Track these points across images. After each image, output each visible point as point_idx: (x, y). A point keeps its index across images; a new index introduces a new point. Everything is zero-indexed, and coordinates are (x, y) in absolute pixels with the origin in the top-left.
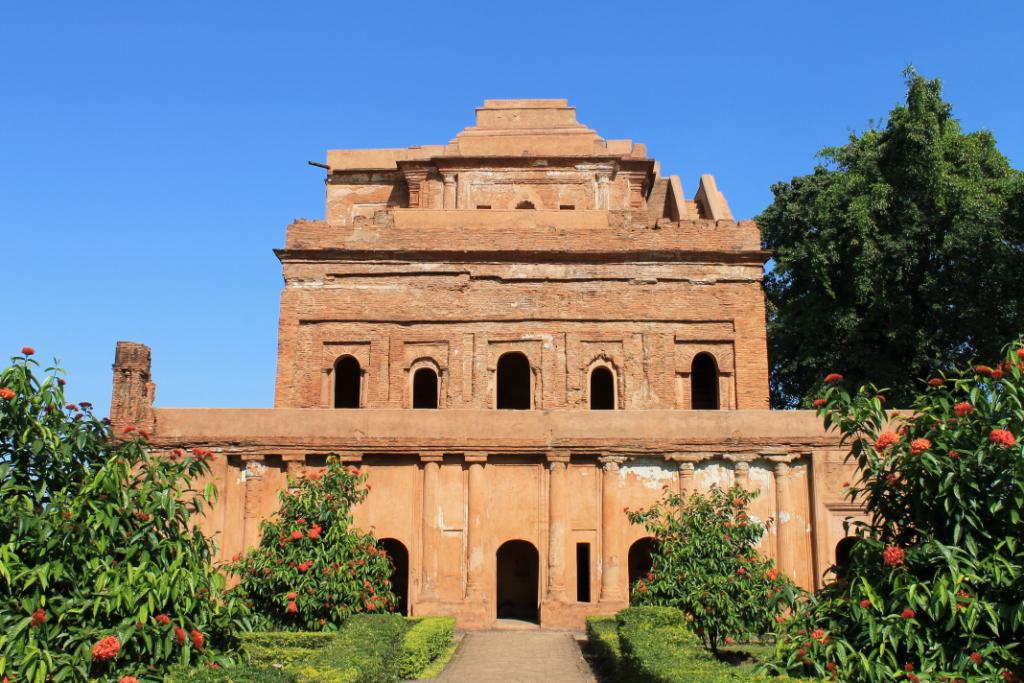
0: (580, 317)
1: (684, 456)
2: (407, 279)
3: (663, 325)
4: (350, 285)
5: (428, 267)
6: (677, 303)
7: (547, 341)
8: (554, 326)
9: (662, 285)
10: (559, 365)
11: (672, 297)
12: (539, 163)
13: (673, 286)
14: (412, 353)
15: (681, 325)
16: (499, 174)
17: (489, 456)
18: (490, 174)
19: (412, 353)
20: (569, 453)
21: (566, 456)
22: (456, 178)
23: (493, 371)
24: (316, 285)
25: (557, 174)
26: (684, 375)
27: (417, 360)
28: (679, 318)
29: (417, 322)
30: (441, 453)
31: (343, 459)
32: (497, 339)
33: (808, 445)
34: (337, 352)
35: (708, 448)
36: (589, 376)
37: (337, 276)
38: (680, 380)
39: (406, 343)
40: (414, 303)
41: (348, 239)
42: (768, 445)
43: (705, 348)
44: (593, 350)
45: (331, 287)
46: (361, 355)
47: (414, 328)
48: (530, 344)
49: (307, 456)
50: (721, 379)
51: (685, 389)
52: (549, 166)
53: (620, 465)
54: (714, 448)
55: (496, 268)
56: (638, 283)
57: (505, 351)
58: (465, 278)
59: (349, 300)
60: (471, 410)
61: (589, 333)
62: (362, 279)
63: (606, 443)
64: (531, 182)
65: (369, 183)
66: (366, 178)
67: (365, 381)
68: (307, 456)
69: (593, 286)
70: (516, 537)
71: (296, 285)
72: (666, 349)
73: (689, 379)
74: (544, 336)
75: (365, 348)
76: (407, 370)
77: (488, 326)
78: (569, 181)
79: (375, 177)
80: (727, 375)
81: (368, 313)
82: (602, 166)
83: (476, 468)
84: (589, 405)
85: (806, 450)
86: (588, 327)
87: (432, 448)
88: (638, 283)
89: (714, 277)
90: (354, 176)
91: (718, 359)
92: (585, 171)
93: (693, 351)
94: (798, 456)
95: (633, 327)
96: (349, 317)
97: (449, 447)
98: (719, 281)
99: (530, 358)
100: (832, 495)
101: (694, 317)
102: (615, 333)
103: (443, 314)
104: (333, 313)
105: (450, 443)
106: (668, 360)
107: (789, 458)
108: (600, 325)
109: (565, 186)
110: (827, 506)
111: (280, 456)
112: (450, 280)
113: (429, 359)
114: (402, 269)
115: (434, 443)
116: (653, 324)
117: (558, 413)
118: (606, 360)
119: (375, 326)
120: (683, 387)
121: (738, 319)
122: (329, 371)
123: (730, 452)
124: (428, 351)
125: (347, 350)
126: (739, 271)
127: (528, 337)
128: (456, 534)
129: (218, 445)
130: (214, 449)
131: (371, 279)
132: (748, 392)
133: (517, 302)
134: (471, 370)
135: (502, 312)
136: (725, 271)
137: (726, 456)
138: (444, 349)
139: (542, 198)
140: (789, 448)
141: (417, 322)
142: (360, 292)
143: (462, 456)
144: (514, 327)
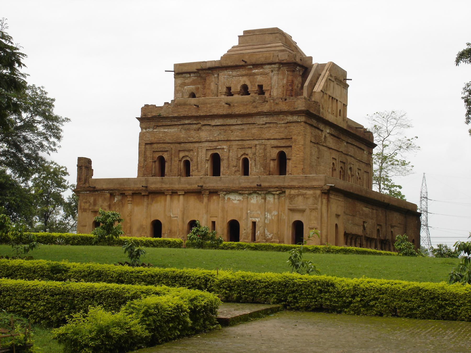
2: (180, 127)
3: (267, 141)
4: (162, 130)
5: (187, 122)
6: (273, 132)
7: (226, 148)
8: (228, 143)
9: (267, 125)
10: (230, 157)
11: (270, 130)
12: (249, 67)
13: (272, 125)
14: (182, 155)
15: (273, 141)
16: (235, 73)
18: (231, 73)
19: (182, 155)
20: (208, 191)
22: (218, 74)
23: (208, 160)
24: (151, 130)
25: (256, 71)
26: (274, 160)
27: (183, 157)
28: (272, 138)
29: (183, 143)
31: (142, 194)
32: (209, 148)
33: (284, 188)
34: (157, 155)
35: (251, 189)
36: (241, 161)
37: (157, 126)
38: (272, 162)
39: (180, 151)
40: (182, 136)
41: (161, 112)
42: (270, 188)
43: (282, 149)
45: (155, 130)
46: (166, 156)
47: (182, 145)
50: (287, 161)
51: (274, 165)
52: (253, 68)
53: (225, 195)
54: (254, 189)
55: (210, 121)
56: (259, 125)
57: (212, 153)
58: (199, 126)
59: (161, 135)
60: (201, 175)
62: (166, 128)
63: (219, 188)
64: (246, 75)
65: (190, 77)
66: (189, 75)
67: (166, 164)
69: (243, 127)
71: (144, 130)
72: (268, 150)
73: (276, 162)
74: (225, 147)
75: (166, 153)
76: (180, 161)
77: (206, 144)
78: (261, 74)
79: (192, 75)
80: (290, 159)
81: (167, 140)
82: (273, 66)
83: (181, 197)
84: (240, 172)
85: (283, 190)
86: (240, 143)
87: (168, 190)
88: (259, 125)
90: (184, 75)
91: (286, 153)
92: (267, 69)
93: (277, 151)
95: (256, 142)
96: (161, 142)
97: (172, 190)
98: (288, 122)
99: (220, 155)
100: (291, 206)
101: (277, 137)
102: (249, 144)
103: (191, 139)
104: (156, 140)
105: (173, 188)
106: (268, 154)
107: (278, 193)
108: (244, 142)
109: (259, 76)
110: (289, 209)
112: (195, 126)
113: (187, 156)
115: (169, 188)
116: (263, 141)
117: (230, 175)
118: (247, 155)
119: (169, 145)
120: (273, 165)
121: (294, 137)
122: (155, 162)
123: (259, 191)
124: (187, 153)
125: (160, 154)
126: (295, 118)
127: (219, 147)
129: (107, 190)
131: (168, 127)
132: (296, 166)
133: (216, 134)
134: (202, 161)
135: (211, 138)
136: (290, 118)
138: (191, 153)
139: (251, 83)
141: (183, 143)
142: (165, 132)
143: (177, 193)
144: (215, 144)
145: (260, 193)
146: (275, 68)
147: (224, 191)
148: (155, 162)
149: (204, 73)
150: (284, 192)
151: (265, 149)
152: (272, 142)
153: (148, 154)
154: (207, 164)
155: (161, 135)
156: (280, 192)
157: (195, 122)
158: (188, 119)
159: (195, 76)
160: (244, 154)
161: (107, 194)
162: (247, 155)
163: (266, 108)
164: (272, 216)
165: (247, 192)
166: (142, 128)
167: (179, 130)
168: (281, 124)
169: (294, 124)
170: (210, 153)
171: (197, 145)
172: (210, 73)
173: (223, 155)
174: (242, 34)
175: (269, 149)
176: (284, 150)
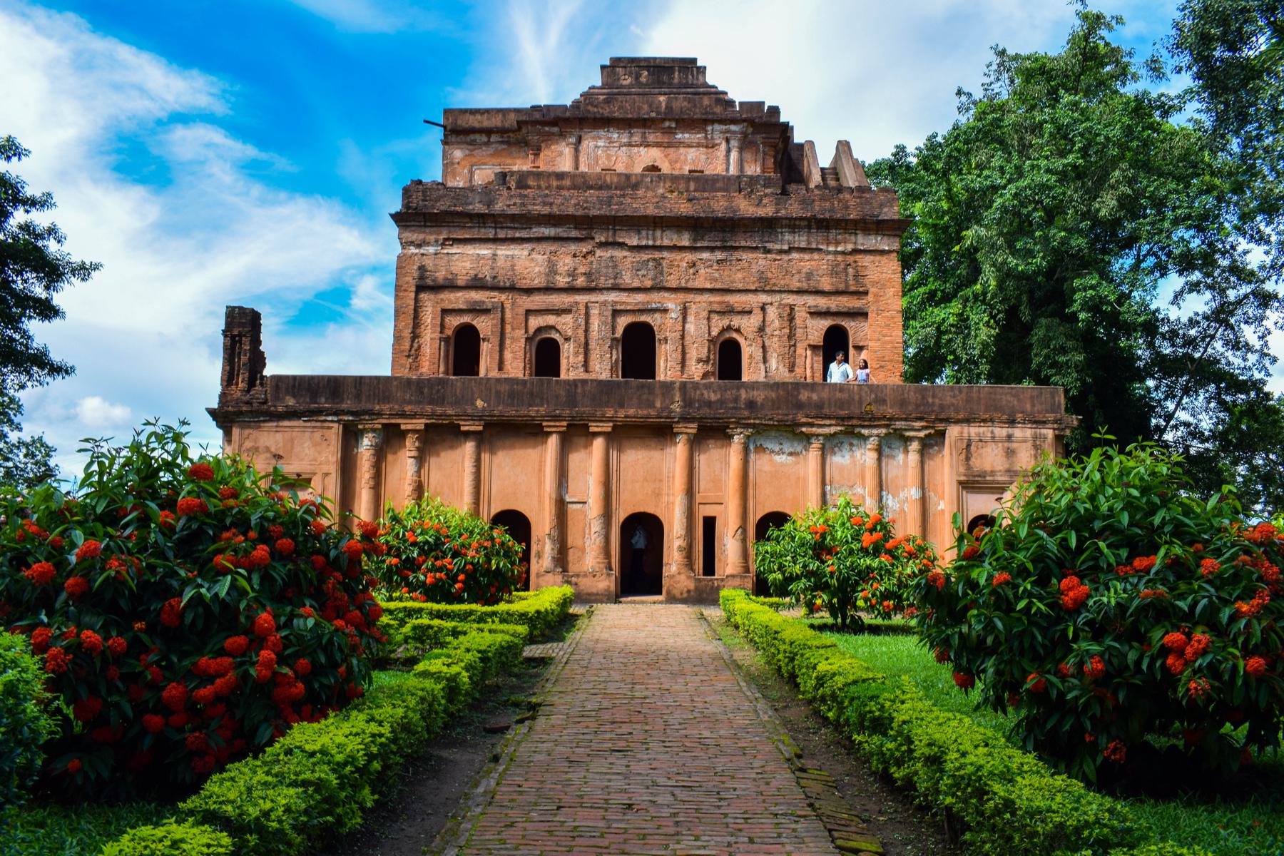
0: (708, 286)
1: (814, 430)
2: (528, 246)
12: (667, 124)
17: (614, 427)
18: (616, 136)
19: (535, 322)
21: (692, 428)
25: (687, 136)
27: (539, 330)
30: (565, 424)
34: (454, 322)
44: (718, 323)
46: (484, 325)
48: (657, 316)
49: (426, 425)
61: (719, 303)
66: (484, 139)
67: (485, 347)
68: (426, 425)
70: (642, 510)
71: (413, 250)
72: (798, 321)
74: (670, 306)
77: (612, 297)
79: (494, 138)
82: (733, 128)
85: (940, 426)
89: (850, 247)
90: (472, 137)
91: (851, 333)
93: (826, 323)
94: (932, 431)
95: (764, 298)
106: (799, 332)
107: (922, 434)
111: (399, 425)
114: (524, 234)
118: (738, 331)
121: (872, 290)
123: (864, 427)
124: (551, 320)
125: (466, 319)
128: (579, 506)
130: (330, 418)
132: (882, 367)
137: (857, 430)
138: (568, 319)
140: (923, 424)
145: (865, 432)
146: (735, 132)
147: (747, 426)
148: (447, 340)
149: (539, 133)
150: (942, 434)
151: (791, 318)
152: (812, 301)
153: (429, 315)
154: (614, 352)
155: (468, 265)
156: (927, 432)
157: (574, 234)
158: (555, 226)
159: (502, 142)
160: (729, 328)
161: (336, 425)
162: (738, 331)
163: (793, 208)
164: (902, 502)
165: (820, 431)
166: (405, 244)
167: (526, 253)
168: (836, 253)
169: (869, 258)
170: (623, 322)
171: (582, 298)
172: (553, 134)
173: (665, 326)
174: (608, 63)
175: (801, 315)
176: (845, 323)
